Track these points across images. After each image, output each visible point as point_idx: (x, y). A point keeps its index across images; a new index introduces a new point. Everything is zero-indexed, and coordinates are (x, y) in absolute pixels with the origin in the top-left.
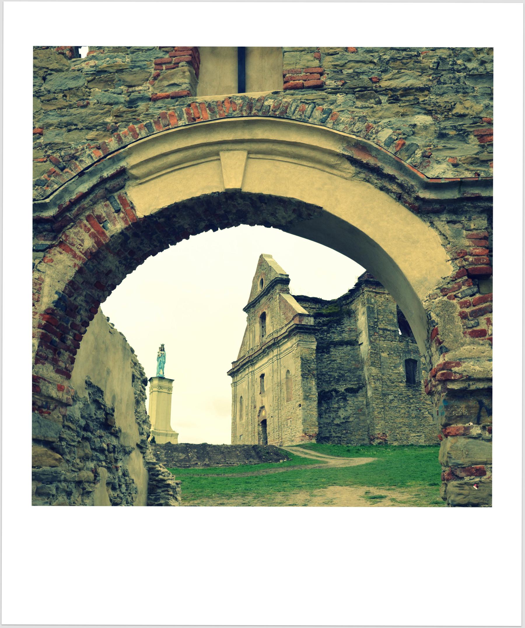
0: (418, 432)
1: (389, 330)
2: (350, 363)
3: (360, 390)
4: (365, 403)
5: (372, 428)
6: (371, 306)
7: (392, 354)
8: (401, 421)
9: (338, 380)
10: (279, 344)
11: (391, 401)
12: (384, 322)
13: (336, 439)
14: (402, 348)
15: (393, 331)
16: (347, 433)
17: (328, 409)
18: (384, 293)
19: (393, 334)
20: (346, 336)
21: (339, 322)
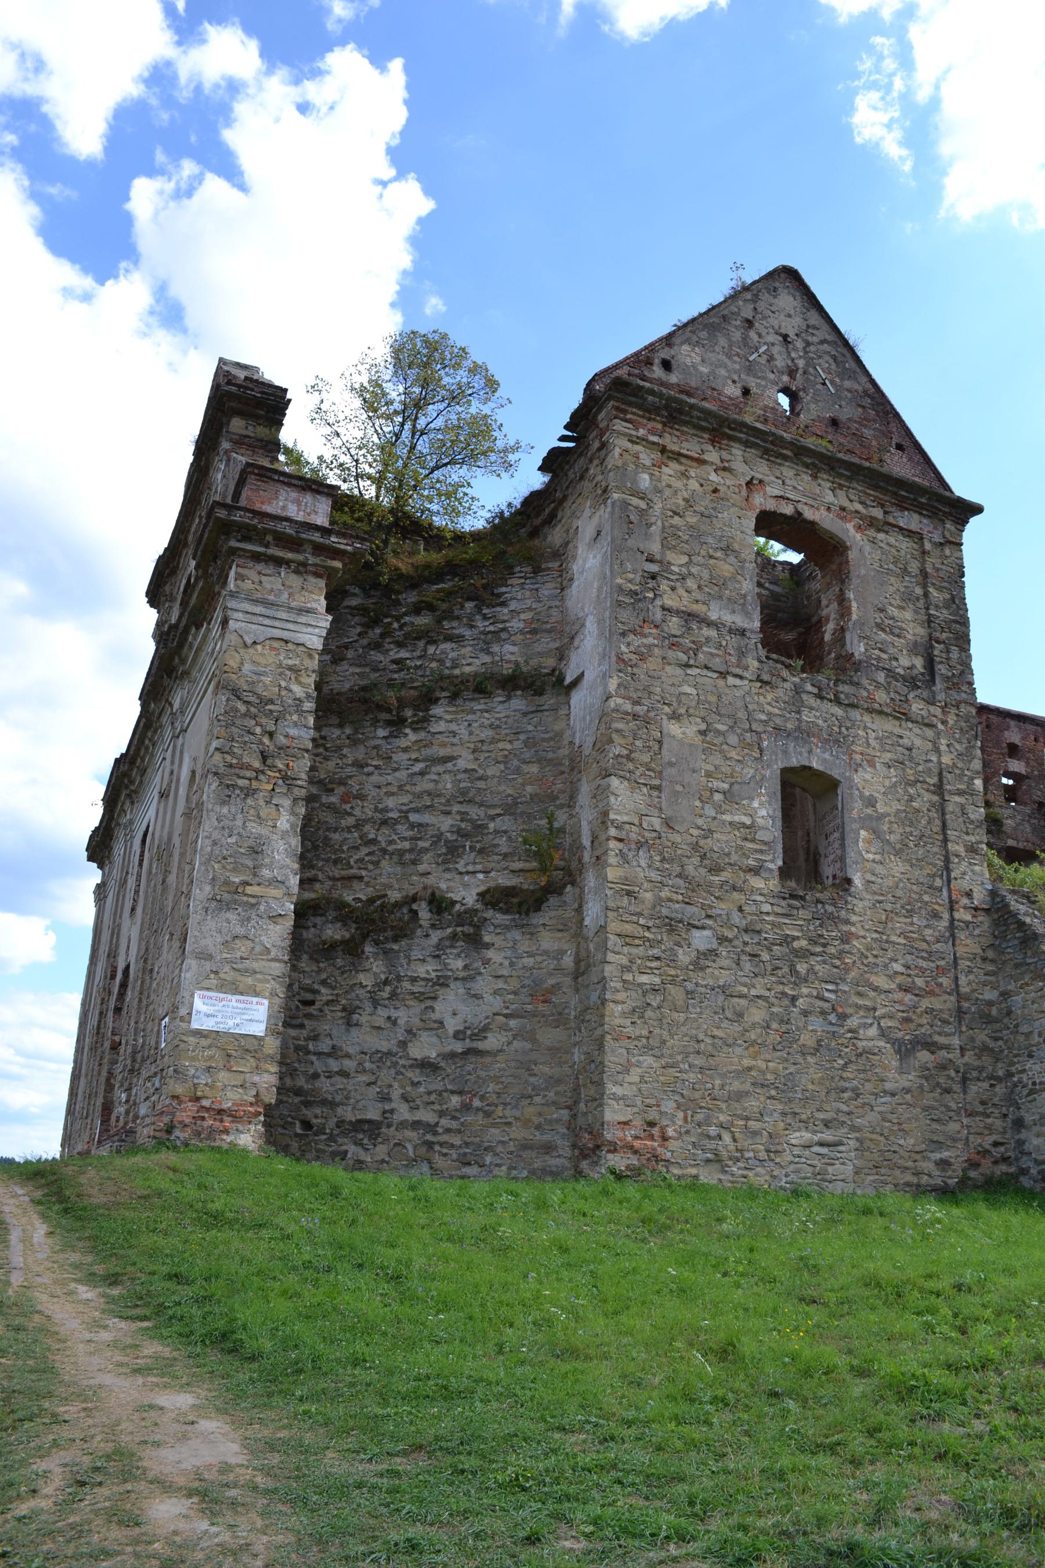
0: (827, 1124)
1: (710, 624)
2: (518, 771)
3: (553, 900)
4: (568, 961)
6: (635, 501)
7: (718, 732)
8: (747, 1062)
9: (453, 851)
10: (183, 661)
11: (704, 958)
12: (691, 583)
13: (409, 1133)
14: (769, 714)
15: (730, 631)
16: (466, 1107)
17: (386, 982)
19: (732, 642)
20: (510, 654)
21: (487, 597)
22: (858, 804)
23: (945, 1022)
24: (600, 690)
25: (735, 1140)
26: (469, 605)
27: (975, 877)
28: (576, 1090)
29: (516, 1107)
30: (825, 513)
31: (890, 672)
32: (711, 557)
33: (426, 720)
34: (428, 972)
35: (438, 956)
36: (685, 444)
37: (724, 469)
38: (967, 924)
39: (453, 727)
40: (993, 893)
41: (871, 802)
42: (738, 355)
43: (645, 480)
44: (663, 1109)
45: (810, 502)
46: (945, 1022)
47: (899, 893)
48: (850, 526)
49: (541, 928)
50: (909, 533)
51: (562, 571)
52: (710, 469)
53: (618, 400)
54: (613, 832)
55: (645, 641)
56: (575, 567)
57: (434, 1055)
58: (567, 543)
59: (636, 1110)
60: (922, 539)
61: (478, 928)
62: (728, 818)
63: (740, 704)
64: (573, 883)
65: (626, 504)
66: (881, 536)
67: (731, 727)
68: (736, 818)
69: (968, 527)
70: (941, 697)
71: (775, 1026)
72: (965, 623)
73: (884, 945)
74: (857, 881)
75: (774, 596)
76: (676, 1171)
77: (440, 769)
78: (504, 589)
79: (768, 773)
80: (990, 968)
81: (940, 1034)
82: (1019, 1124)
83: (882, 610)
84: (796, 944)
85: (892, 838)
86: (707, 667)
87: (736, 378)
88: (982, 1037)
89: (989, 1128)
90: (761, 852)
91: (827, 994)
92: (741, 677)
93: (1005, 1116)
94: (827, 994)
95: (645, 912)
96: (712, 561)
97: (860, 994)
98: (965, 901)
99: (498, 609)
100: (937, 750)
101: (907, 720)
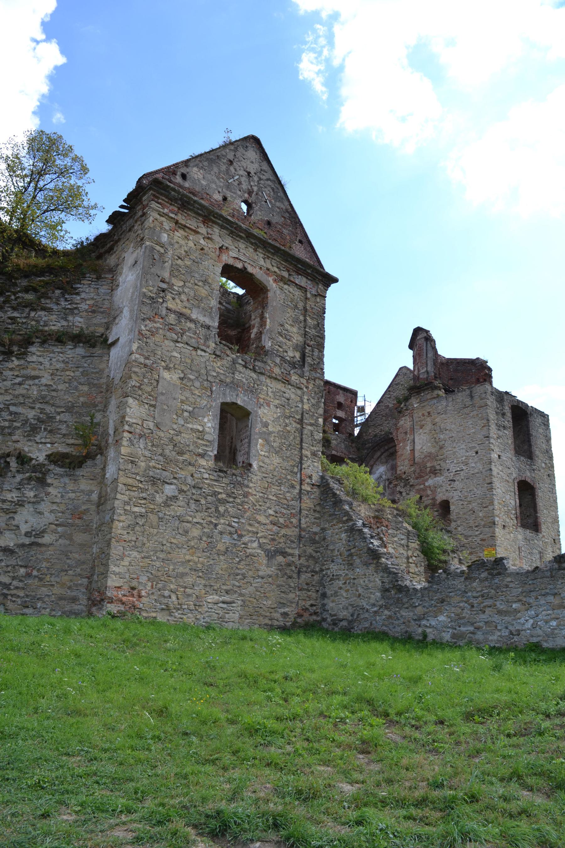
0: (227, 592)
1: (191, 320)
2: (76, 388)
3: (89, 463)
4: (95, 497)
5: (102, 569)
6: (158, 248)
7: (190, 379)
8: (187, 557)
9: (34, 430)
12: (183, 297)
14: (218, 373)
15: (202, 326)
16: (29, 575)
18: (197, 232)
19: (202, 332)
20: (78, 322)
21: (69, 289)
22: (259, 425)
23: (292, 542)
24: (127, 349)
25: (178, 599)
26: (58, 292)
27: (314, 468)
28: (93, 568)
29: (58, 576)
30: (259, 270)
31: (283, 358)
32: (196, 284)
33: (25, 353)
34: (12, 498)
35: (19, 489)
36: (189, 221)
37: (208, 238)
38: (308, 492)
39: (41, 359)
40: (322, 478)
41: (266, 425)
42: (223, 178)
43: (165, 237)
44: (140, 581)
45: (251, 263)
46: (292, 542)
47: (275, 474)
48: (271, 279)
49: (81, 477)
50: (300, 287)
51: (113, 280)
52: (201, 237)
53: (154, 190)
54: (126, 427)
55: (155, 325)
56: (120, 279)
57: (12, 545)
58: (118, 265)
59: (125, 580)
60: (306, 291)
61: (44, 474)
62: (190, 426)
63: (203, 365)
64: (102, 454)
65: (153, 249)
66: (286, 287)
67: (197, 377)
68: (195, 427)
69: (330, 288)
70: (307, 374)
71: (204, 539)
72: (323, 337)
73: (265, 500)
74: (255, 465)
75: (227, 310)
76: (145, 614)
77: (31, 382)
78: (79, 286)
79: (214, 404)
80: (317, 515)
81: (289, 548)
82: (324, 595)
83: (282, 325)
84: (220, 496)
85: (275, 445)
86: (187, 344)
87: (220, 190)
88: (310, 550)
89: (309, 597)
90: (206, 446)
91: (233, 524)
92: (205, 351)
93: (318, 591)
94: (233, 524)
95: (141, 473)
96: (196, 287)
97: (250, 525)
98: (308, 480)
99: (74, 296)
100: (302, 401)
101: (289, 384)
